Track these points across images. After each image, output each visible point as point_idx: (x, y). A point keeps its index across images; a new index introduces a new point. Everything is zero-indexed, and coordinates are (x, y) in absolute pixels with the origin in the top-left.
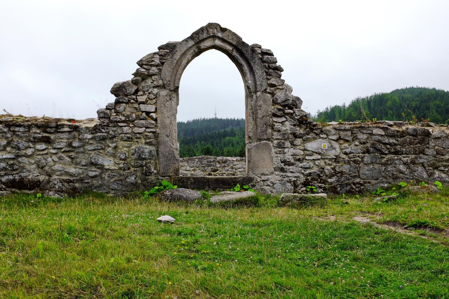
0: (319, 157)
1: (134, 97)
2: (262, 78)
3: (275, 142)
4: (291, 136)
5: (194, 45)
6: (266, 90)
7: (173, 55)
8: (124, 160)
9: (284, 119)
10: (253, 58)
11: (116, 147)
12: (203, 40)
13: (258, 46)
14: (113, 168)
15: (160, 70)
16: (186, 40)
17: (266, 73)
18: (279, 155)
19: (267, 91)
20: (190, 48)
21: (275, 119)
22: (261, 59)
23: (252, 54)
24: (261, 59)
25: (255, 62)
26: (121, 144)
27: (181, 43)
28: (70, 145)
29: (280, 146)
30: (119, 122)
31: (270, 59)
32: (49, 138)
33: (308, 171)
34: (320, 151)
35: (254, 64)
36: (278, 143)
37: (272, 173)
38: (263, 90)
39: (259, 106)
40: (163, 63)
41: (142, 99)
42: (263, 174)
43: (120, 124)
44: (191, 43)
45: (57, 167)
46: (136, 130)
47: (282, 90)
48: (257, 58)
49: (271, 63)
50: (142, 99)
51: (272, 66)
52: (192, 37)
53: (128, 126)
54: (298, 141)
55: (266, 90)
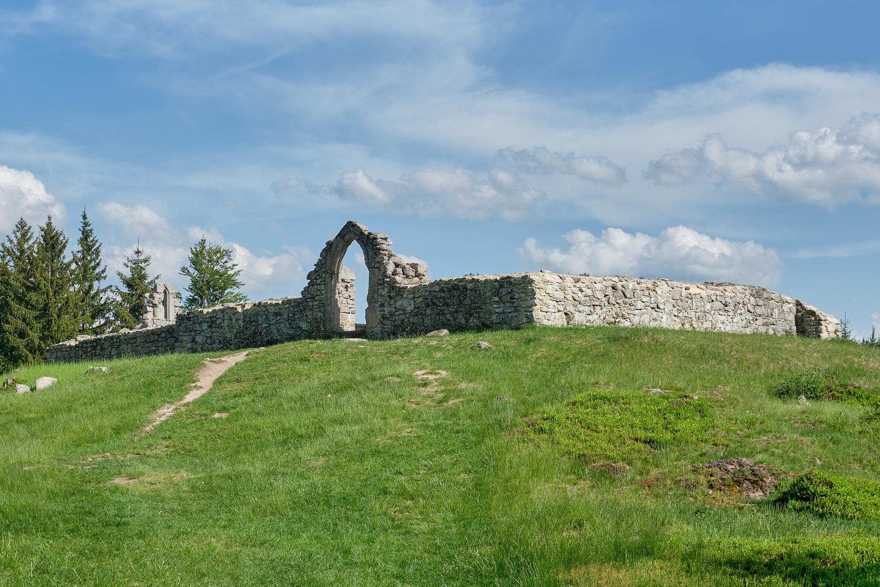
0: (402, 312)
1: (315, 281)
3: (379, 303)
4: (388, 299)
6: (374, 265)
8: (310, 323)
9: (383, 286)
10: (368, 243)
11: (307, 315)
12: (345, 235)
14: (305, 329)
15: (326, 260)
16: (336, 237)
18: (381, 313)
19: (375, 266)
20: (339, 242)
21: (380, 287)
26: (309, 313)
28: (288, 316)
29: (382, 305)
30: (308, 299)
32: (280, 312)
33: (396, 323)
34: (402, 308)
36: (381, 304)
37: (377, 326)
38: (372, 266)
40: (327, 255)
41: (319, 281)
42: (372, 327)
43: (308, 300)
45: (285, 330)
46: (315, 303)
50: (319, 281)
52: (339, 234)
53: (312, 301)
54: (392, 302)
55: (374, 265)
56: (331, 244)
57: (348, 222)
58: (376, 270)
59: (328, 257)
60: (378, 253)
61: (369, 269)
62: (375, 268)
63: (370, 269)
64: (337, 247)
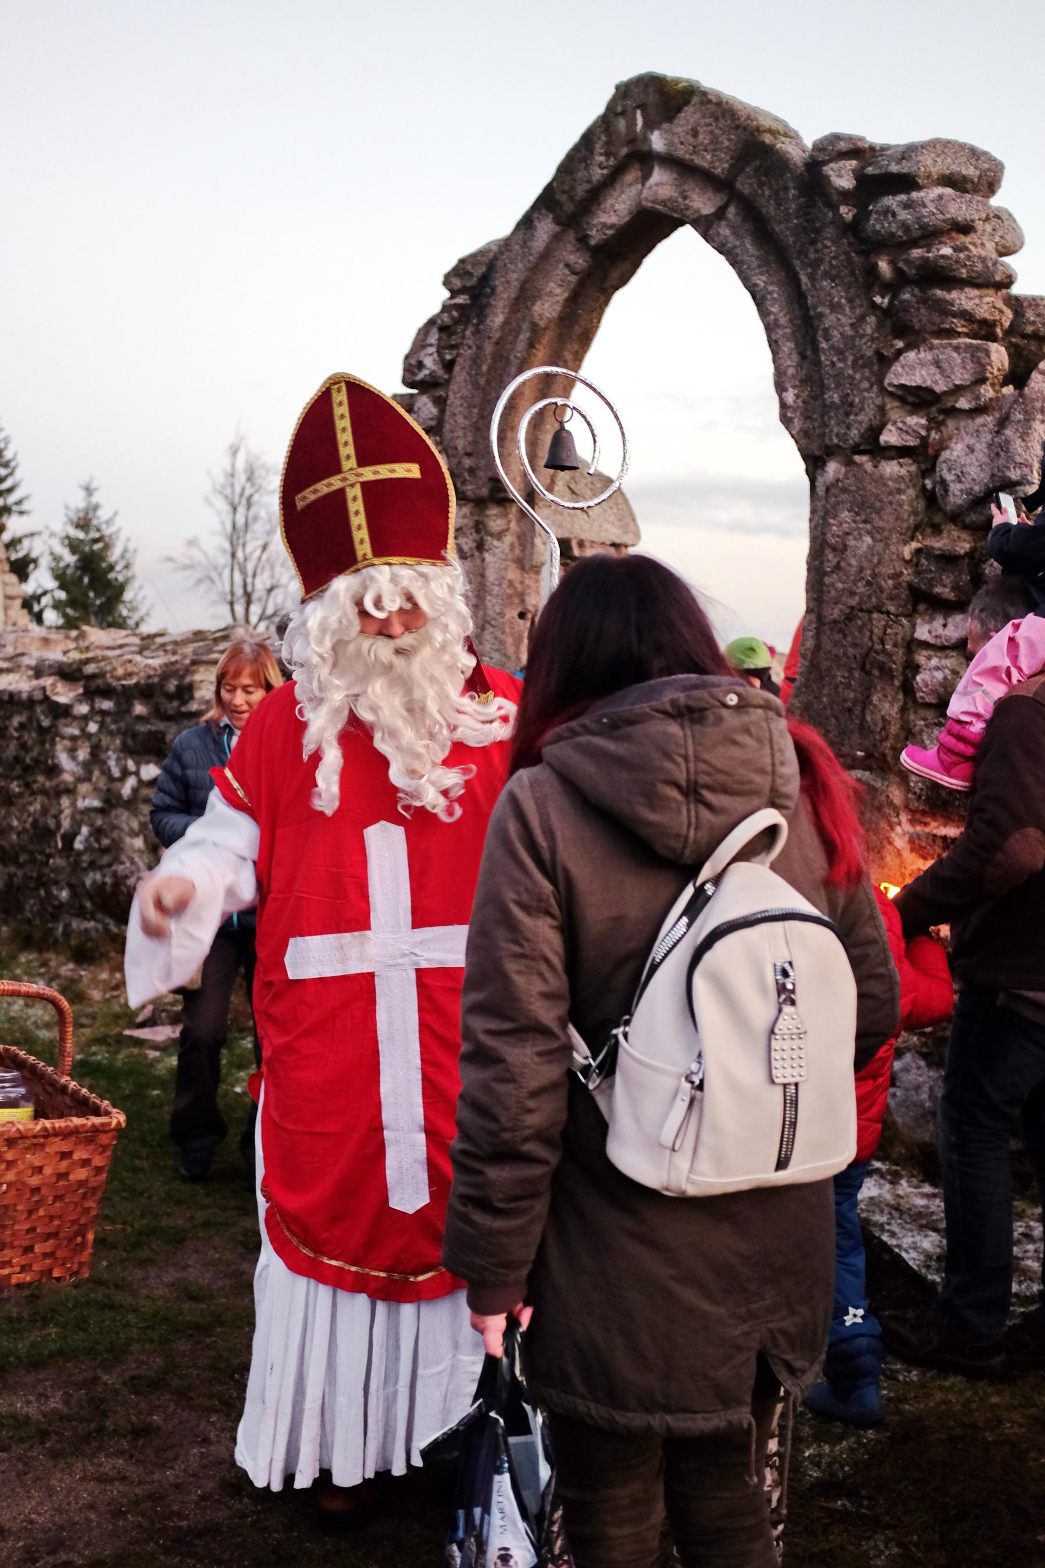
2: (855, 362)
5: (556, 238)
7: (482, 317)
10: (811, 231)
12: (597, 194)
13: (842, 146)
16: (527, 223)
17: (886, 314)
19: (890, 437)
20: (546, 255)
22: (854, 229)
23: (806, 211)
24: (854, 229)
25: (816, 264)
27: (506, 244)
31: (903, 215)
35: (812, 277)
39: (834, 549)
40: (449, 366)
44: (545, 228)
47: (980, 420)
48: (829, 232)
49: (914, 243)
51: (907, 262)
52: (547, 201)
55: (876, 431)
56: (485, 280)
57: (624, 91)
58: (891, 468)
59: (460, 375)
60: (921, 317)
61: (814, 464)
62: (881, 452)
63: (833, 468)
64: (525, 297)
